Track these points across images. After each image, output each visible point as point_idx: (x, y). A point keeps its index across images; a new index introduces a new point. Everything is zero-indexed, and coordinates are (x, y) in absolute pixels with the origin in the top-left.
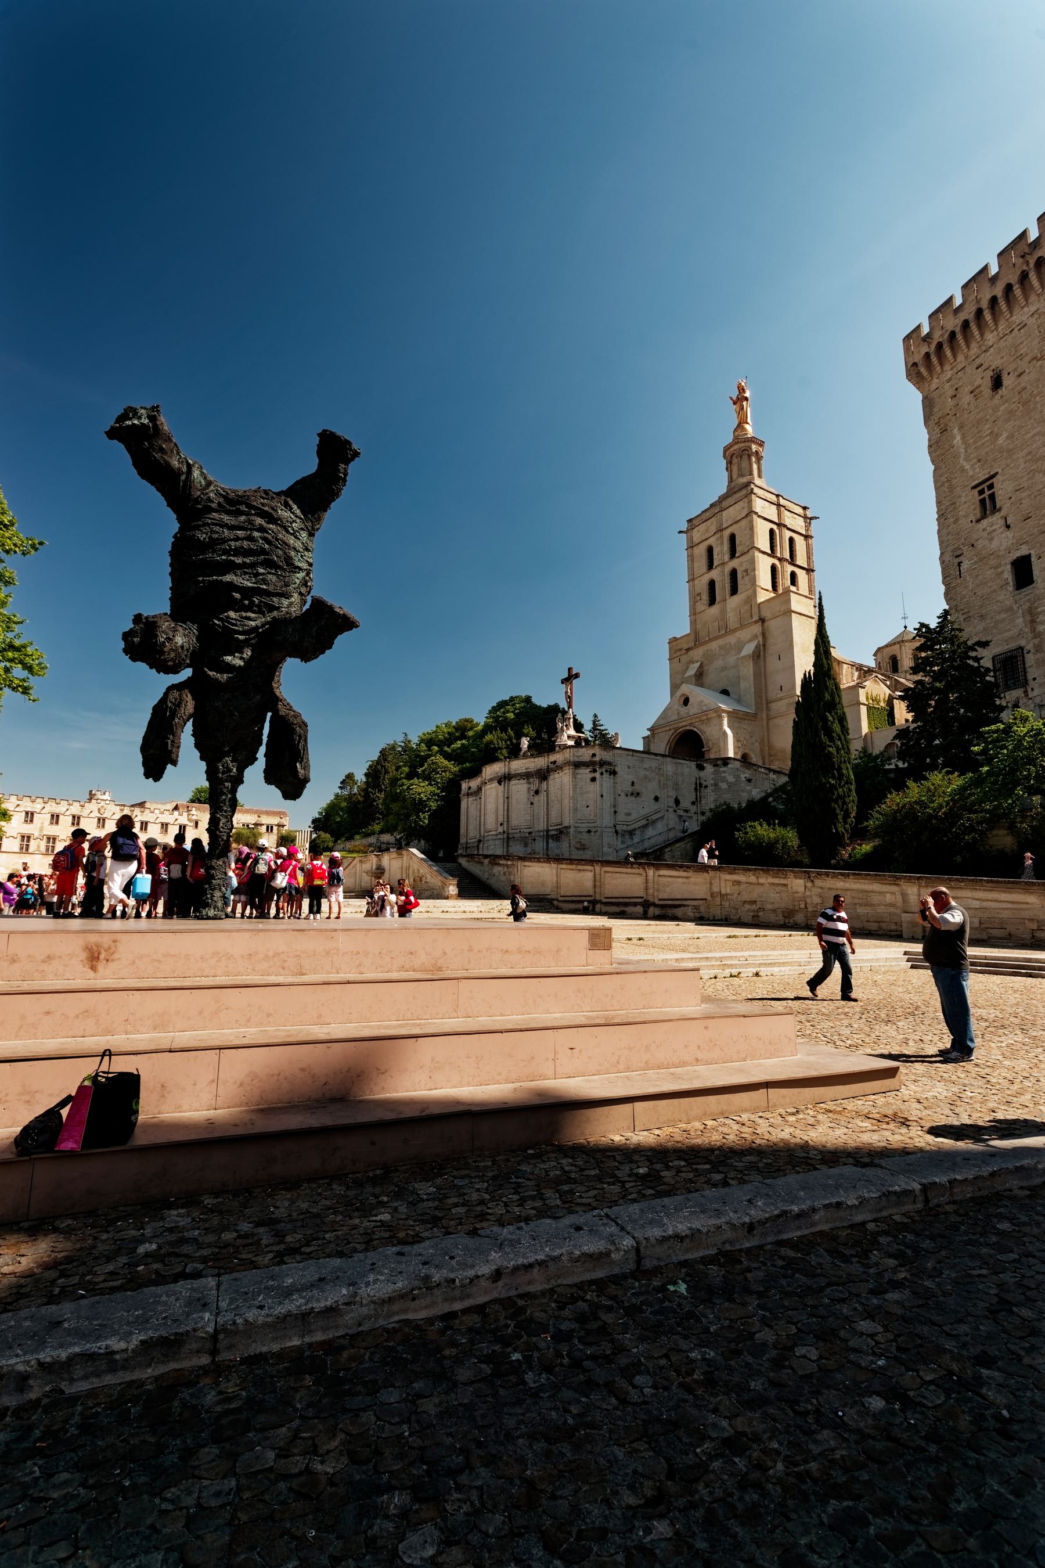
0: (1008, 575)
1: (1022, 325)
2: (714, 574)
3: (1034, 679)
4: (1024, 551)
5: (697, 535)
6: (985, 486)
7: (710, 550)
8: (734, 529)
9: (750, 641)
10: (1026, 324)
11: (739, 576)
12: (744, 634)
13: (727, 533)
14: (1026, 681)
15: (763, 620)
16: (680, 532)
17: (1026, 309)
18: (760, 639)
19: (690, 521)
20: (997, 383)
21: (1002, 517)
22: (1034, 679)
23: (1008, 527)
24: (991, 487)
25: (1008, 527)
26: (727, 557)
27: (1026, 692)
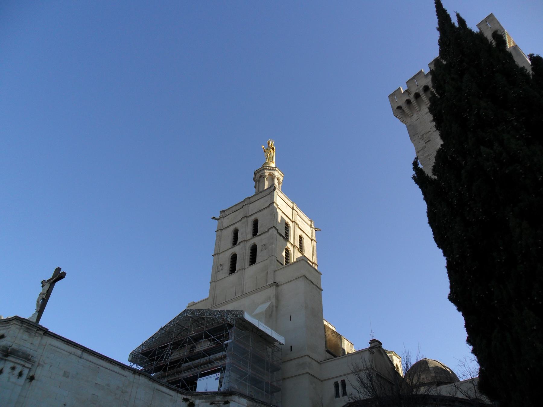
2: (237, 249)
5: (226, 222)
7: (236, 233)
9: (263, 302)
11: (258, 250)
12: (258, 297)
13: (251, 220)
15: (276, 284)
16: (214, 218)
18: (274, 300)
19: (223, 212)
26: (250, 235)
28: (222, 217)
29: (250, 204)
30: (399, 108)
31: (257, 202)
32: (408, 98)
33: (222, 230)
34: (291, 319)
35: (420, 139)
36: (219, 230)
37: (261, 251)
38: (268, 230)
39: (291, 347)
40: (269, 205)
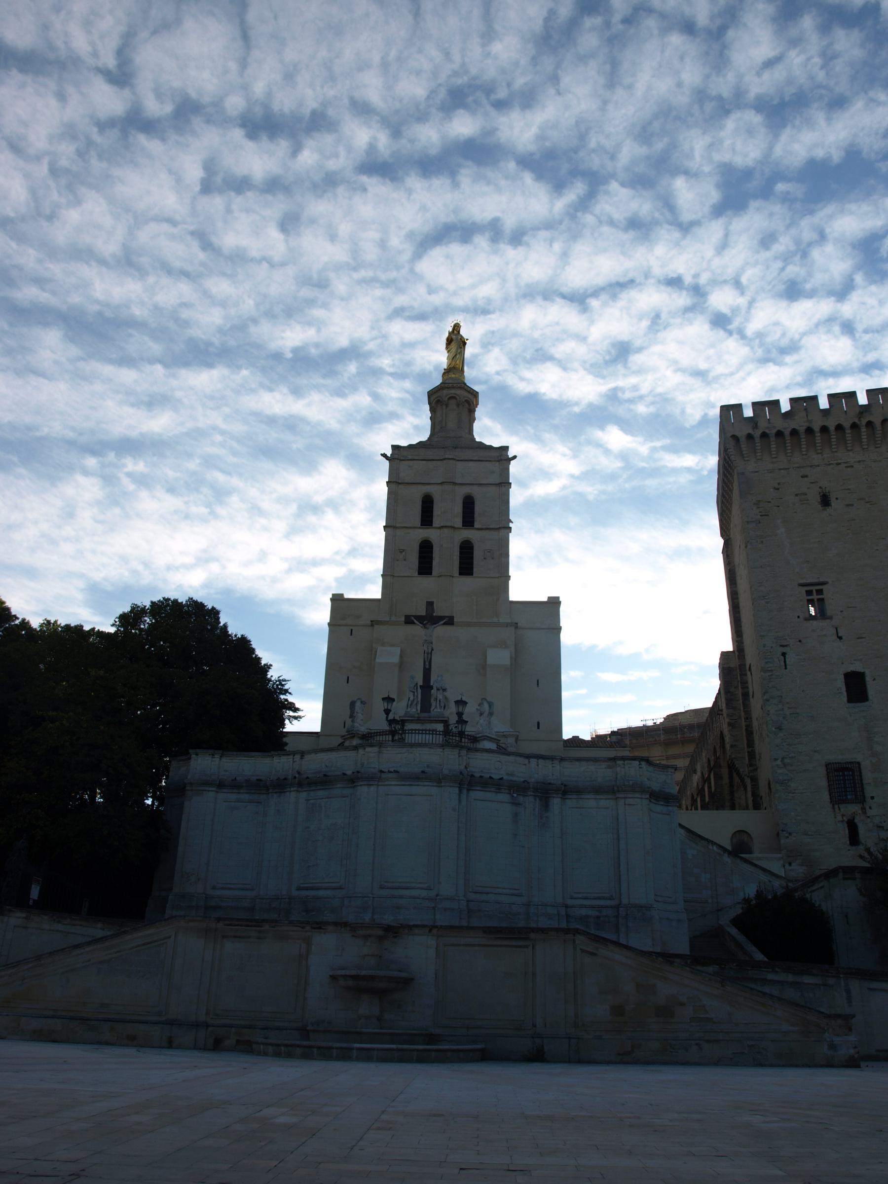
0: (841, 684)
1: (849, 465)
3: (872, 798)
4: (857, 667)
6: (814, 588)
8: (474, 491)
10: (852, 466)
11: (477, 554)
14: (864, 797)
15: (516, 626)
16: (384, 455)
17: (851, 453)
19: (394, 448)
20: (825, 501)
21: (833, 626)
22: (872, 798)
23: (840, 638)
24: (820, 592)
25: (840, 638)
26: (458, 522)
27: (863, 809)
28: (398, 459)
29: (458, 460)
30: (735, 438)
31: (471, 462)
32: (751, 431)
33: (399, 483)
34: (538, 684)
35: (754, 504)
36: (394, 482)
37: (485, 558)
38: (499, 528)
39: (538, 724)
40: (501, 483)
